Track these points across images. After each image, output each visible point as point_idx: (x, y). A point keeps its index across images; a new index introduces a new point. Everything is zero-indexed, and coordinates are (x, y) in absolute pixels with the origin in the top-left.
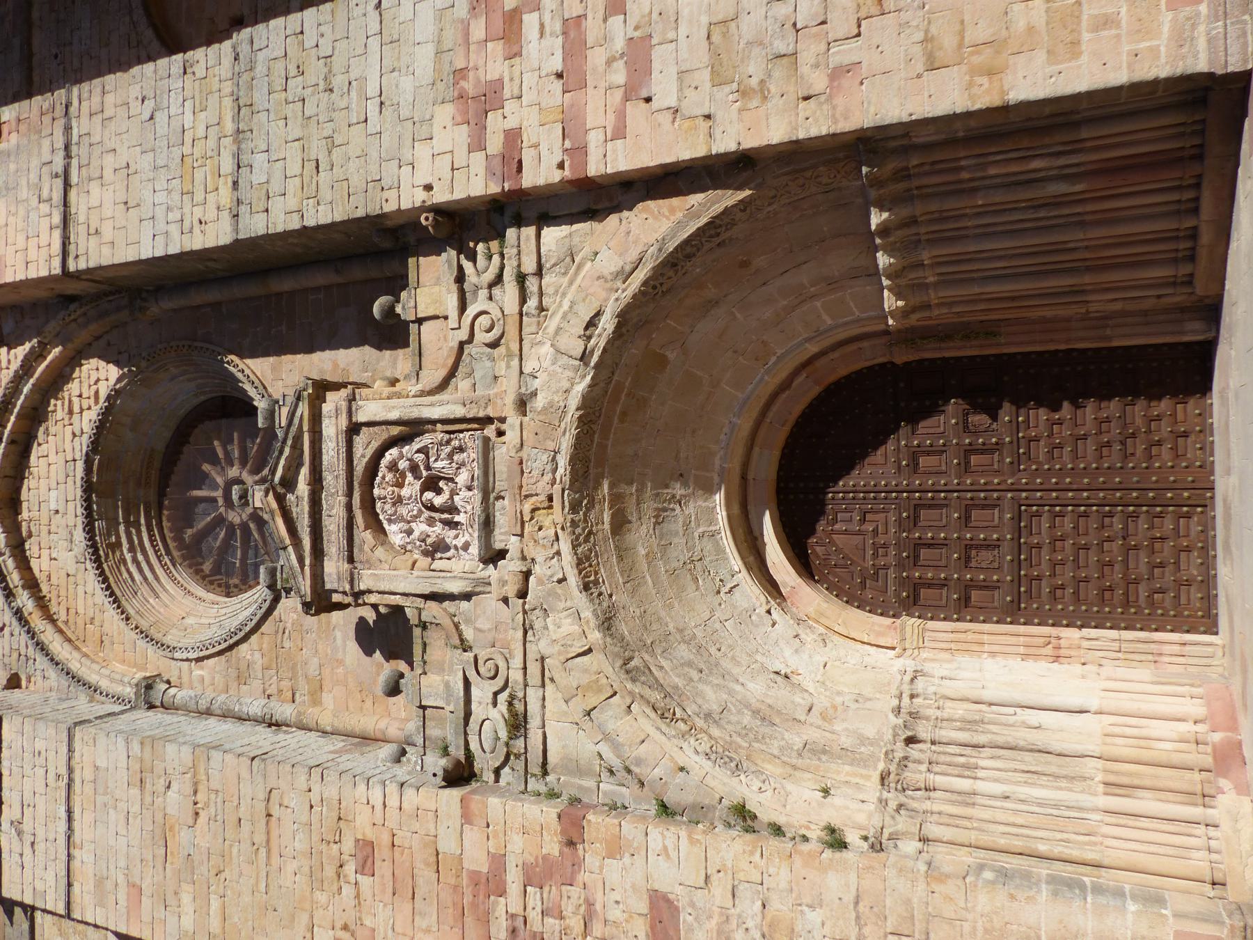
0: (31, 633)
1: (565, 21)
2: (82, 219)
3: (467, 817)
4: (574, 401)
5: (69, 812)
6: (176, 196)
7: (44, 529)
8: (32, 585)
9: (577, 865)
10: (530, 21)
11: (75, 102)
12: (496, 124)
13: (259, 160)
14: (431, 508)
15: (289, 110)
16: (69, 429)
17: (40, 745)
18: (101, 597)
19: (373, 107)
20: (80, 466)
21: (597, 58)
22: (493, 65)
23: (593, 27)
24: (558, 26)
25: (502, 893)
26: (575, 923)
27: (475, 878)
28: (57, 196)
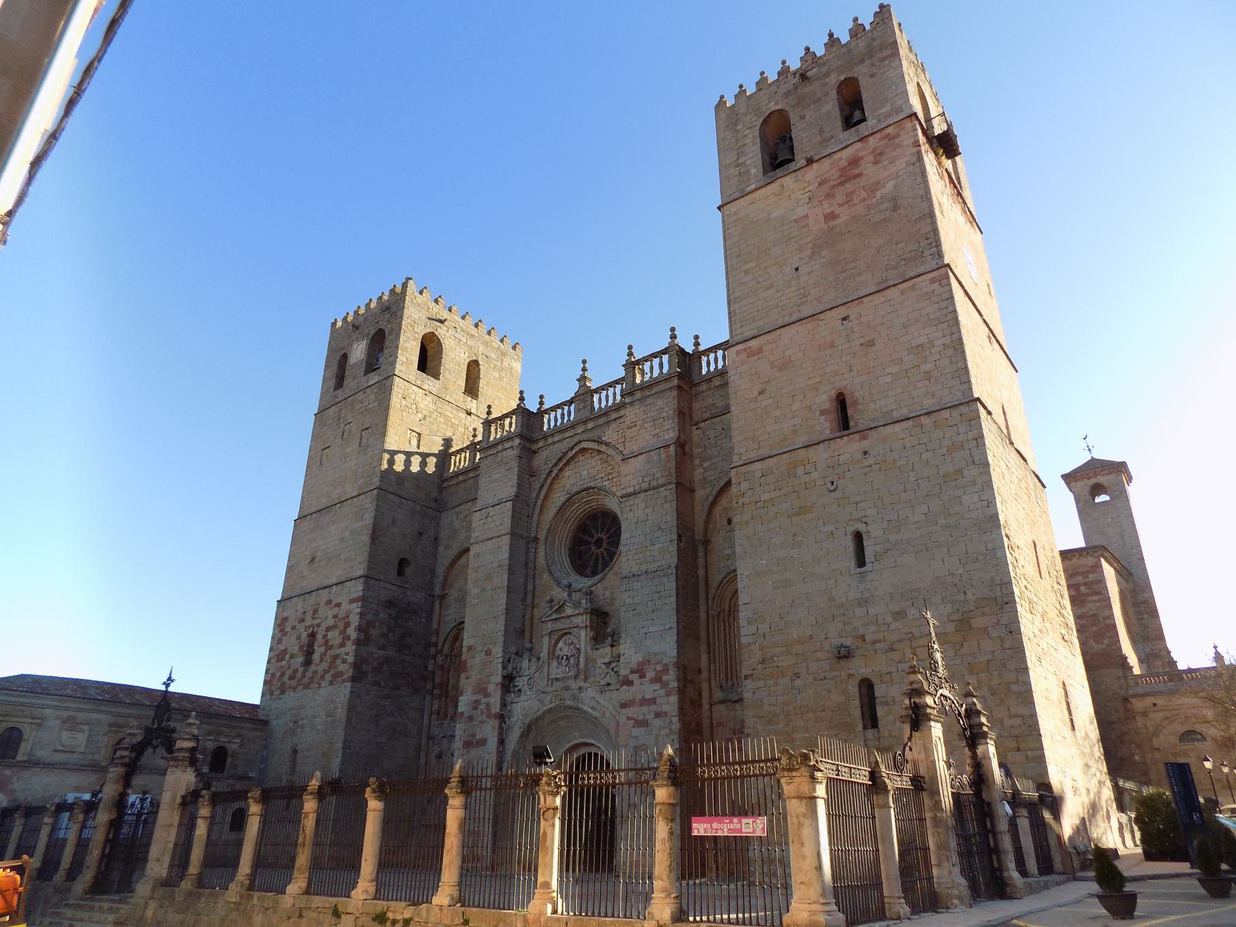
0: (546, 479)
1: (655, 699)
2: (637, 501)
3: (497, 685)
4: (581, 706)
5: (491, 538)
6: (636, 547)
7: (575, 470)
8: (561, 470)
9: (490, 718)
10: (657, 686)
11: (670, 487)
12: (635, 677)
13: (639, 584)
14: (562, 658)
15: (650, 595)
16: (602, 475)
17: (506, 519)
18: (559, 504)
19: (645, 630)
20: (592, 484)
21: (645, 709)
22: (650, 674)
23: (653, 708)
24: (655, 696)
25: (485, 697)
26: (480, 719)
27: (486, 689)
28: (645, 486)
